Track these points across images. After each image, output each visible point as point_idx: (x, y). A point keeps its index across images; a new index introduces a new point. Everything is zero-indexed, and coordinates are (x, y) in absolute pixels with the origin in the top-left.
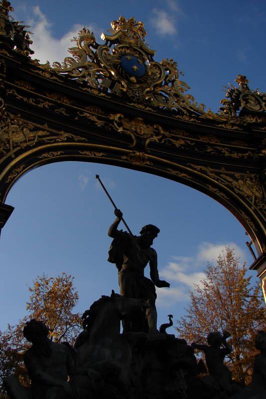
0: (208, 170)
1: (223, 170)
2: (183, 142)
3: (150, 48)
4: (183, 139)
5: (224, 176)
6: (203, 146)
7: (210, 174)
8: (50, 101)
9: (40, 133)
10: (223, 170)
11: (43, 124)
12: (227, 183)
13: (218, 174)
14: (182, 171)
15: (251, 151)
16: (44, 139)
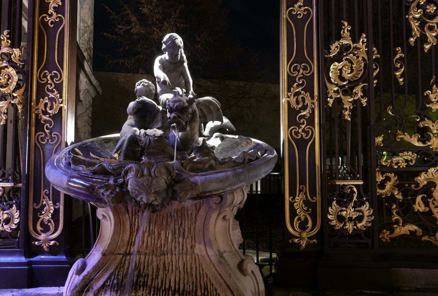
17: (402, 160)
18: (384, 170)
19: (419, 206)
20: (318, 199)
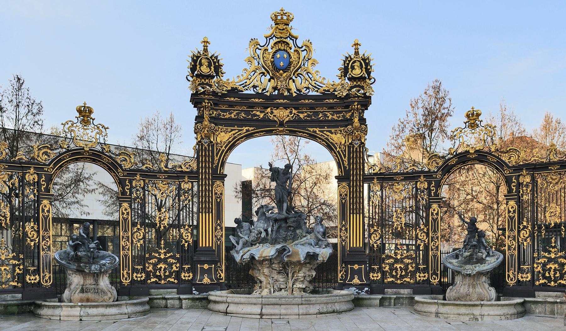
0: (317, 130)
1: (326, 129)
2: (306, 114)
3: (294, 33)
4: (306, 112)
5: (325, 132)
7: (318, 132)
8: (236, 110)
9: (234, 132)
10: (326, 129)
12: (326, 136)
13: (322, 132)
14: (304, 133)
16: (236, 135)
20: (130, 272)
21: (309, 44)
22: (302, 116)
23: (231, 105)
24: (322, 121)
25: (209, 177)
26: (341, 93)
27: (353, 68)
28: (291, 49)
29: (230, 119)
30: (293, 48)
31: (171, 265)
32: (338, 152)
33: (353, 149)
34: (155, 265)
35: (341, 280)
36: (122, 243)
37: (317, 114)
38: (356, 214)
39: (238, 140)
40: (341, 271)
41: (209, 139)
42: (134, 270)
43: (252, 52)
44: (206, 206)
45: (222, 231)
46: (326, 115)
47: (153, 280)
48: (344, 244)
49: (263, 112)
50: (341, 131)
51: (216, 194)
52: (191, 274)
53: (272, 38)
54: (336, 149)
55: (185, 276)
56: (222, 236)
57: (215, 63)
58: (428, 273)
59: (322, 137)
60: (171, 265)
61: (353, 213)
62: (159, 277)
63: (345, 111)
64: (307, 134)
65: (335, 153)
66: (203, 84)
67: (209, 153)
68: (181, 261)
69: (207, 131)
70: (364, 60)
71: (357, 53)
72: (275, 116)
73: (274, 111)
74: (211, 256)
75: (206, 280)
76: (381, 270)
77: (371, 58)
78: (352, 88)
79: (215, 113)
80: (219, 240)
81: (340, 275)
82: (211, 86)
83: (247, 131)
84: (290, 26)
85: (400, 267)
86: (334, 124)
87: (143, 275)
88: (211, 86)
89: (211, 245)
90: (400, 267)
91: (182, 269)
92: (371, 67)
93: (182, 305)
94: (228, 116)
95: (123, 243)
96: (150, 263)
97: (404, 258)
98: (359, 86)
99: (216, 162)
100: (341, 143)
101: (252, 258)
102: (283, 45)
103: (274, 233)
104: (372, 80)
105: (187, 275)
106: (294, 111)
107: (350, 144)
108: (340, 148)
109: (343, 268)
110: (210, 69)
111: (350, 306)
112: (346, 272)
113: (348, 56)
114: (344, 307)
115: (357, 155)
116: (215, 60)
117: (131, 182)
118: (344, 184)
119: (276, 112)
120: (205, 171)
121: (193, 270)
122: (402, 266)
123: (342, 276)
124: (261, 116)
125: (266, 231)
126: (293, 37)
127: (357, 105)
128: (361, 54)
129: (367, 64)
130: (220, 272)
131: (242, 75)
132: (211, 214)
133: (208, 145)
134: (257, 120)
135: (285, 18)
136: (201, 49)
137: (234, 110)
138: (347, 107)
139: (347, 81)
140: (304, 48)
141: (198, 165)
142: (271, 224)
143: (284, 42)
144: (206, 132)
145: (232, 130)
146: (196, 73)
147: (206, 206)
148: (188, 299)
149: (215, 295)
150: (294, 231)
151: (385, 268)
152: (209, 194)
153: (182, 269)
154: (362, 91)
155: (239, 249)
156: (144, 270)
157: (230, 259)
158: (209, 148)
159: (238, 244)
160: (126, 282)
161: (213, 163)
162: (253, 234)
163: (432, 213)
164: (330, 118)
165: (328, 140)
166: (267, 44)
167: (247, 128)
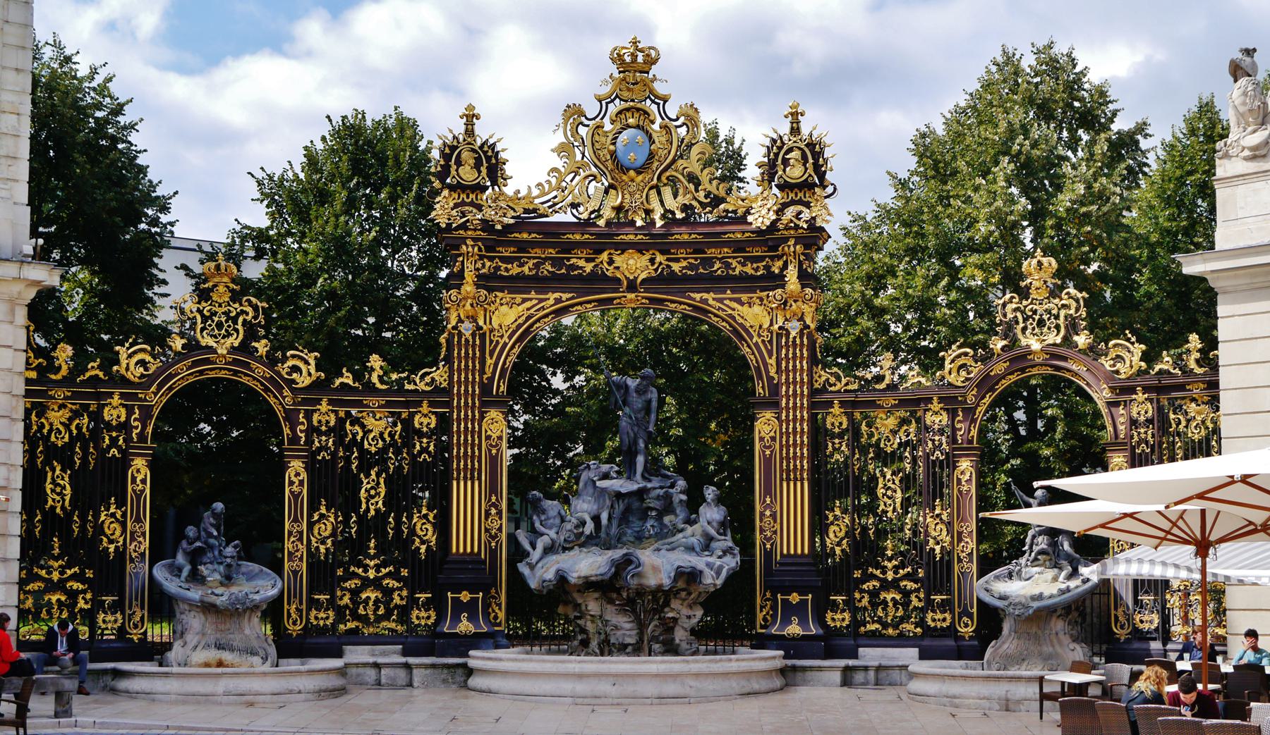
0: (709, 297)
2: (684, 264)
3: (660, 88)
4: (685, 259)
6: (708, 262)
7: (711, 302)
9: (528, 304)
11: (529, 293)
12: (730, 312)
13: (721, 301)
14: (681, 303)
15: (770, 257)
16: (532, 311)
17: (351, 584)
18: (343, 589)
19: (361, 611)
21: (691, 112)
22: (676, 267)
23: (523, 247)
24: (720, 279)
25: (474, 403)
26: (760, 220)
27: (786, 162)
28: (653, 122)
29: (520, 277)
30: (659, 120)
31: (388, 592)
32: (756, 344)
33: (787, 338)
34: (355, 593)
35: (762, 627)
36: (288, 545)
37: (708, 262)
38: (796, 479)
39: (538, 320)
40: (762, 608)
41: (475, 321)
42: (313, 604)
43: (569, 134)
44: (466, 464)
45: (501, 518)
46: (728, 266)
47: (351, 625)
48: (768, 546)
49: (593, 260)
50: (761, 299)
51: (488, 438)
52: (433, 614)
53: (612, 101)
54: (751, 337)
55: (422, 617)
56: (500, 529)
57: (488, 159)
58: (952, 612)
59: (720, 313)
60: (388, 592)
61: (788, 480)
62: (364, 619)
63: (770, 257)
64: (689, 305)
65: (749, 346)
66: (463, 204)
67: (474, 351)
68: (412, 585)
69: (472, 305)
70: (811, 145)
71: (795, 130)
72: (617, 268)
73: (616, 258)
74: (477, 573)
75: (465, 626)
76: (850, 605)
77: (826, 140)
78: (785, 206)
79: (488, 264)
80: (493, 537)
81: (760, 616)
82: (480, 208)
83: (558, 301)
84: (651, 76)
85: (893, 599)
86: (746, 284)
87: (331, 613)
88: (480, 208)
89: (476, 550)
90: (893, 599)
91: (412, 602)
92: (826, 161)
93: (411, 679)
94: (515, 270)
95: (290, 546)
96: (346, 589)
97: (902, 579)
98: (800, 202)
99: (489, 371)
100: (761, 327)
101: (562, 579)
102: (636, 115)
103: (615, 523)
104: (830, 190)
105: (423, 614)
106: (660, 258)
107: (780, 328)
108: (759, 335)
109: (768, 600)
110: (479, 172)
111: (778, 682)
112: (774, 608)
113: (775, 136)
114: (764, 684)
115: (795, 354)
116: (490, 153)
117: (309, 415)
118: (769, 415)
119: (619, 260)
120: (466, 390)
121: (437, 604)
122: (898, 597)
123: (765, 619)
124: (588, 270)
125: (596, 519)
126: (656, 97)
127: (795, 245)
128: (805, 131)
129: (817, 155)
130: (497, 610)
131: (549, 182)
132: (476, 483)
133: (473, 335)
134: (580, 278)
135: (640, 59)
136: (459, 129)
137: (529, 258)
138: (775, 248)
139: (775, 190)
140: (682, 120)
141: (451, 377)
142: (608, 503)
143: (638, 110)
144: (468, 307)
145: (524, 301)
146: (448, 181)
147: (466, 464)
148: (426, 666)
149: (477, 659)
150: (659, 518)
151: (860, 601)
152: (473, 440)
153: (412, 602)
154: (806, 215)
155: (534, 561)
156: (332, 603)
157: (516, 580)
158: (474, 341)
159: (534, 548)
160: (294, 629)
161: (482, 372)
162: (569, 526)
163: (959, 481)
164: (737, 272)
165: (733, 318)
166: (602, 114)
167: (557, 295)
